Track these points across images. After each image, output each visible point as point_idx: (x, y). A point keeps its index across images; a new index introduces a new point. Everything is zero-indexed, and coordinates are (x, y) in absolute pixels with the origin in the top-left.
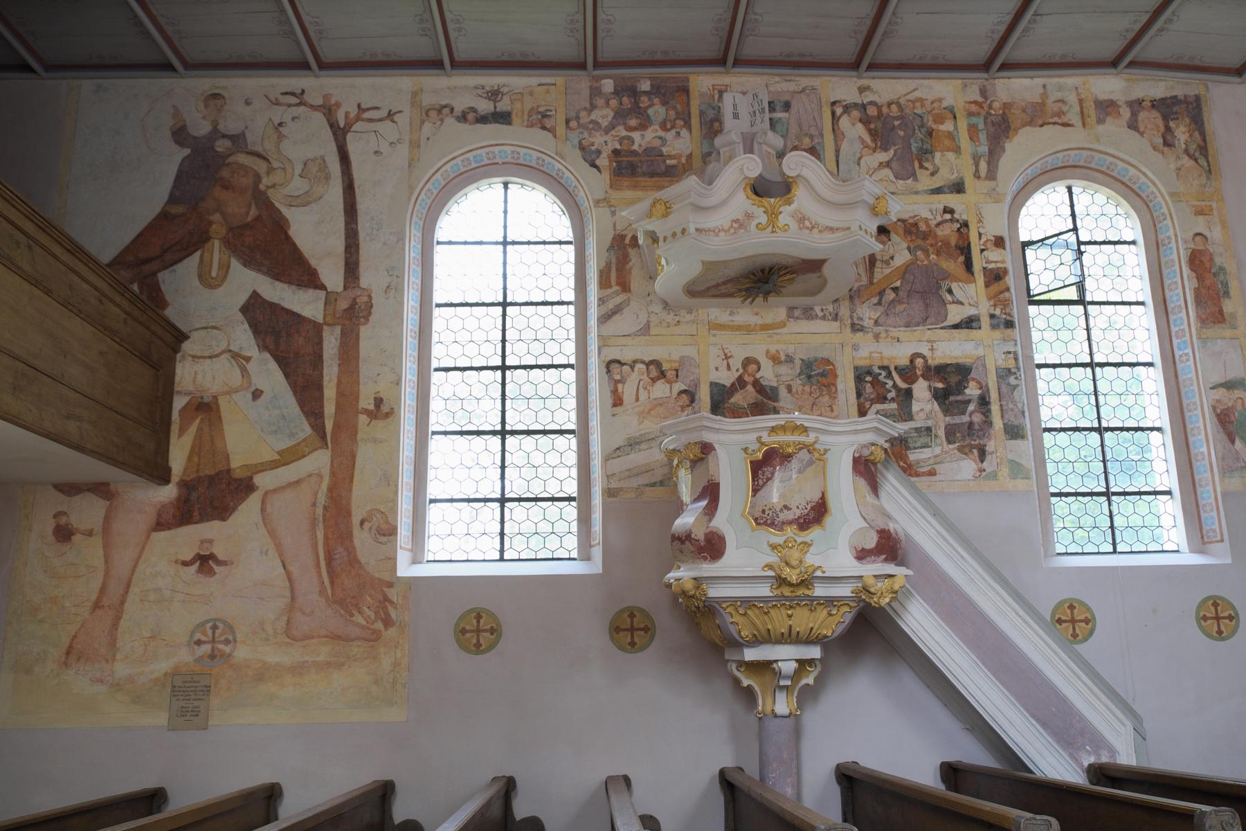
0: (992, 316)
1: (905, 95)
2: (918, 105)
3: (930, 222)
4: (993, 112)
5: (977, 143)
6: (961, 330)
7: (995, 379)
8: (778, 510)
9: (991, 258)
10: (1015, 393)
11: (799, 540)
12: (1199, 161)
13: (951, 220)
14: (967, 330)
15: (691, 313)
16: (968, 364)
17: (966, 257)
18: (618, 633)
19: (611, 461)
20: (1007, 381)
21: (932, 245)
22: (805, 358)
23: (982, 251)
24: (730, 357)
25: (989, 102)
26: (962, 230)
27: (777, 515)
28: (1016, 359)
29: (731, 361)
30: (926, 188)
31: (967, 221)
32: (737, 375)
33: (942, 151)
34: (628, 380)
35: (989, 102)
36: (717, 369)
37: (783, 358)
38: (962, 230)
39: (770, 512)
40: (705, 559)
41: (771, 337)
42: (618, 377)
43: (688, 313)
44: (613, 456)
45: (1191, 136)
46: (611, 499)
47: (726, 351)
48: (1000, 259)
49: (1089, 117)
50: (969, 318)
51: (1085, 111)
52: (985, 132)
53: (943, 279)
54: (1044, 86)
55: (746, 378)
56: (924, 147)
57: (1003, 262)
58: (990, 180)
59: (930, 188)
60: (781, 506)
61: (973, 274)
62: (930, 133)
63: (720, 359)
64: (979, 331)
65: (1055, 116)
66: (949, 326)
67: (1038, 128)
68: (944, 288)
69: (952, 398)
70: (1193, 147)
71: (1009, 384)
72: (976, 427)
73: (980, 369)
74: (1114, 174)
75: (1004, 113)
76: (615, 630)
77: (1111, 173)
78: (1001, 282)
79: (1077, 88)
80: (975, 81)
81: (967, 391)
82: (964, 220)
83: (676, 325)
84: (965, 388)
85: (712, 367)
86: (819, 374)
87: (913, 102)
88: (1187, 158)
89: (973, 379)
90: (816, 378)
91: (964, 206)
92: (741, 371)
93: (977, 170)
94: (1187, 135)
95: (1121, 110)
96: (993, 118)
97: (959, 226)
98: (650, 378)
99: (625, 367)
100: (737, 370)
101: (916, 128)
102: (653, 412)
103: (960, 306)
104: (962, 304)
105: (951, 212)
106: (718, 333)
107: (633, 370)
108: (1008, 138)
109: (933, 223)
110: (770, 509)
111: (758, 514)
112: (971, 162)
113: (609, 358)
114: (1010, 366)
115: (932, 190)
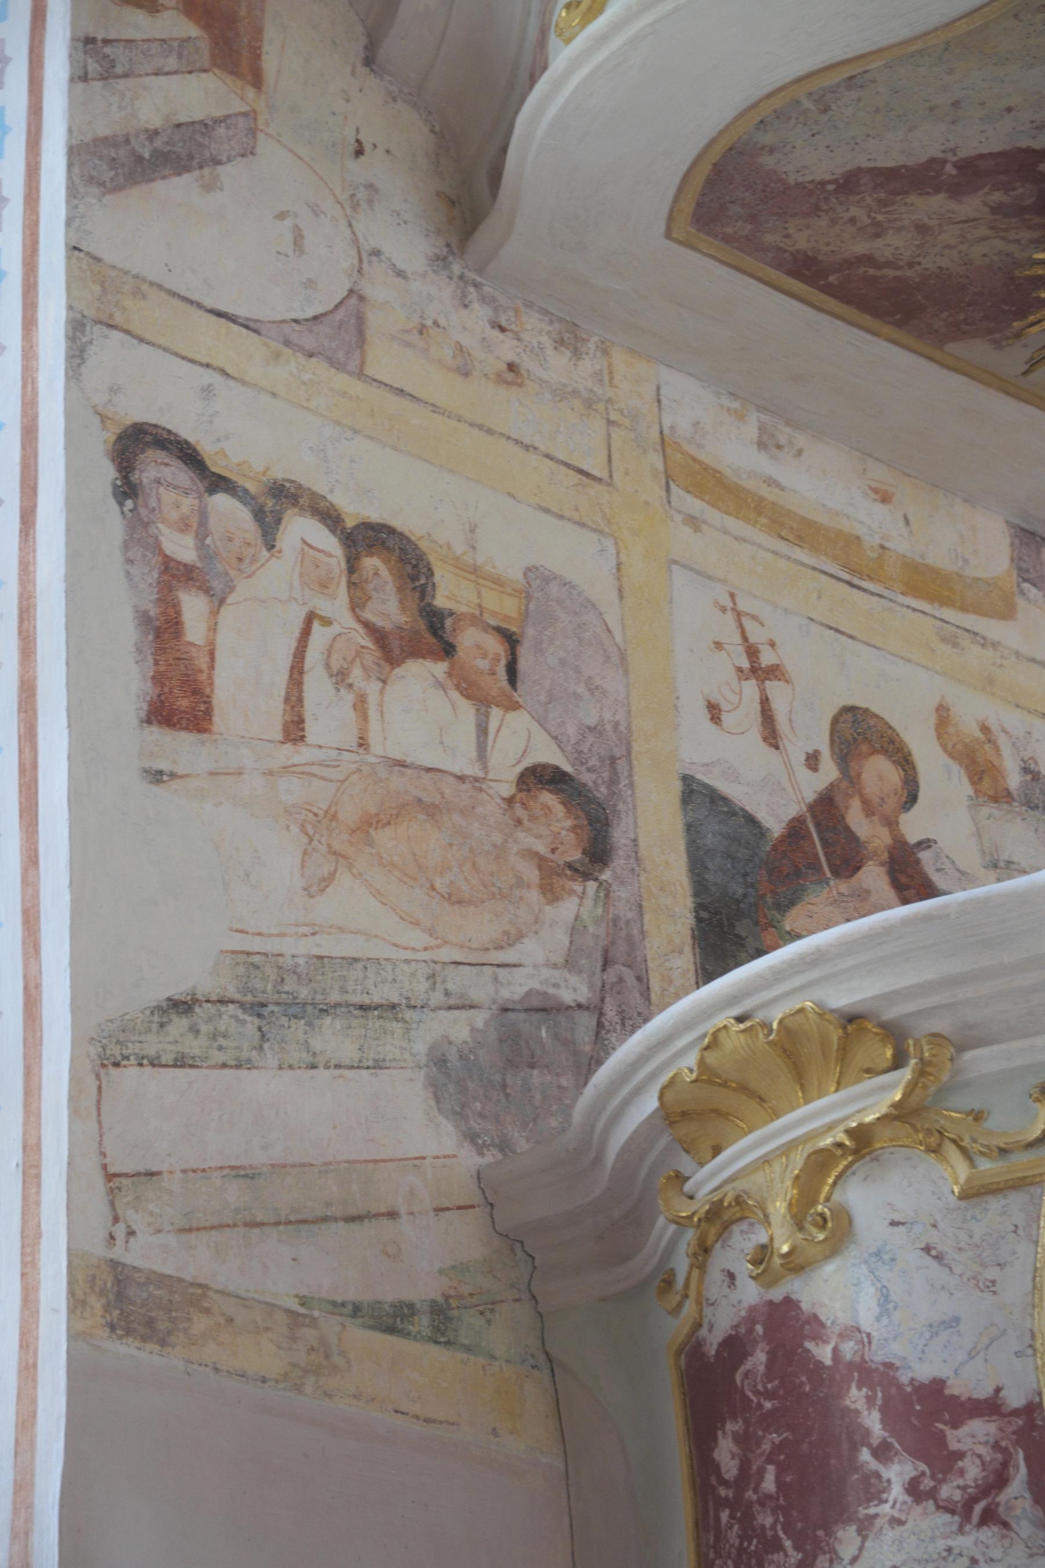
15: (577, 354)
19: (130, 1076)
29: (774, 688)
36: (714, 713)
37: (1014, 780)
41: (951, 641)
43: (560, 342)
44: (152, 1045)
46: (127, 1349)
47: (756, 635)
83: (500, 379)
92: (829, 772)
98: (367, 625)
99: (221, 501)
100: (812, 761)
102: (384, 837)
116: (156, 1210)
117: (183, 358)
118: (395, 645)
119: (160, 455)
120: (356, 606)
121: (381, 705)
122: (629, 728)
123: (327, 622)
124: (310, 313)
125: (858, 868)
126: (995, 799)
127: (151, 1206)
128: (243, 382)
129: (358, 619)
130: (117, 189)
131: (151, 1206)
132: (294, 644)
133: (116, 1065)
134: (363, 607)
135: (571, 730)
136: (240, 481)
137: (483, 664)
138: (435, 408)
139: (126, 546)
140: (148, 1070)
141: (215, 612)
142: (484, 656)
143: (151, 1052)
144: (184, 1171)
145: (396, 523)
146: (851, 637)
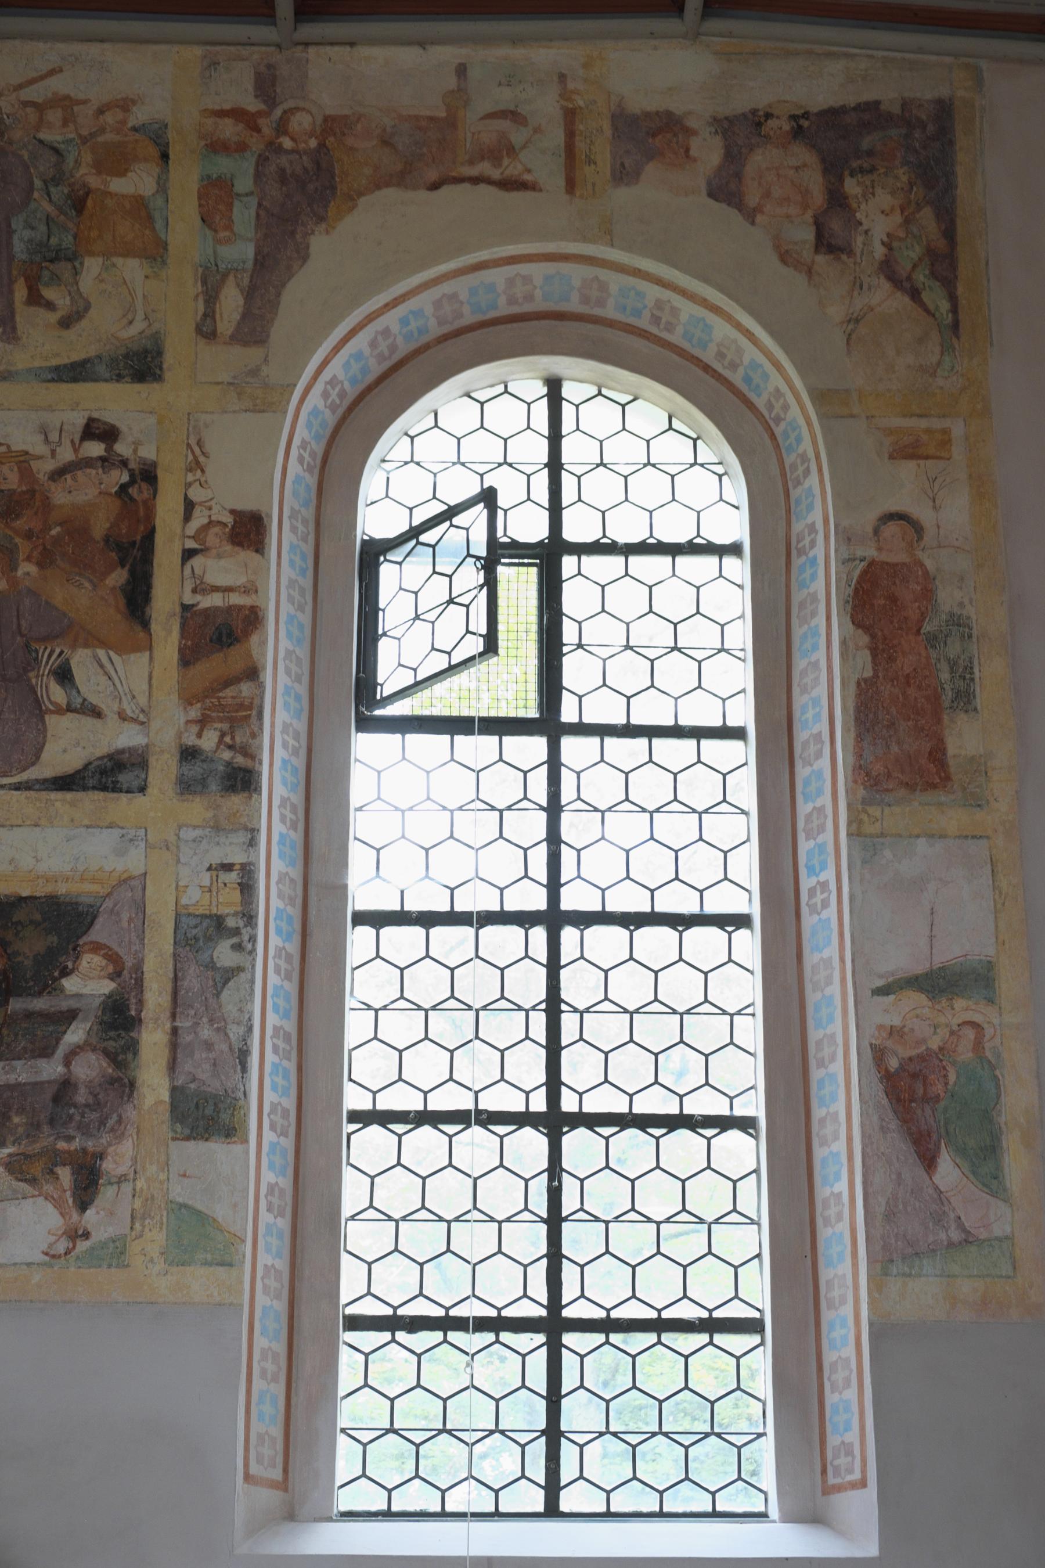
0: (189, 754)
1: (20, 87)
2: (54, 116)
3: (35, 465)
4: (287, 143)
5: (223, 234)
6: (80, 795)
7: (169, 949)
9: (211, 579)
10: (225, 994)
12: (925, 296)
13: (103, 459)
14: (100, 795)
16: (83, 899)
17: (132, 573)
20: (205, 957)
21: (29, 535)
23: (188, 554)
25: (278, 112)
26: (133, 491)
28: (247, 888)
30: (37, 364)
31: (154, 465)
33: (107, 254)
35: (278, 112)
38: (133, 491)
45: (907, 221)
48: (241, 580)
49: (590, 161)
50: (110, 757)
51: (580, 145)
52: (254, 201)
53: (45, 639)
54: (461, 70)
56: (54, 241)
57: (250, 589)
58: (245, 344)
59: (54, 362)
61: (145, 624)
62: (79, 201)
64: (139, 799)
65: (483, 158)
66: (45, 781)
67: (423, 195)
68: (48, 661)
69: (16, 1004)
70: (910, 254)
71: (211, 966)
72: (82, 1097)
73: (125, 916)
74: (675, 338)
75: (322, 145)
77: (665, 335)
78: (235, 651)
79: (562, 78)
80: (245, 51)
81: (70, 984)
82: (143, 462)
84: (65, 973)
87: (40, 108)
88: (886, 285)
89: (97, 948)
91: (152, 420)
93: (209, 314)
94: (898, 218)
95: (695, 144)
96: (284, 161)
97: (125, 478)
101: (38, 183)
103: (89, 722)
104: (96, 713)
105: (109, 434)
108: (321, 219)
109: (43, 468)
112: (193, 287)
114: (223, 910)
115: (57, 369)
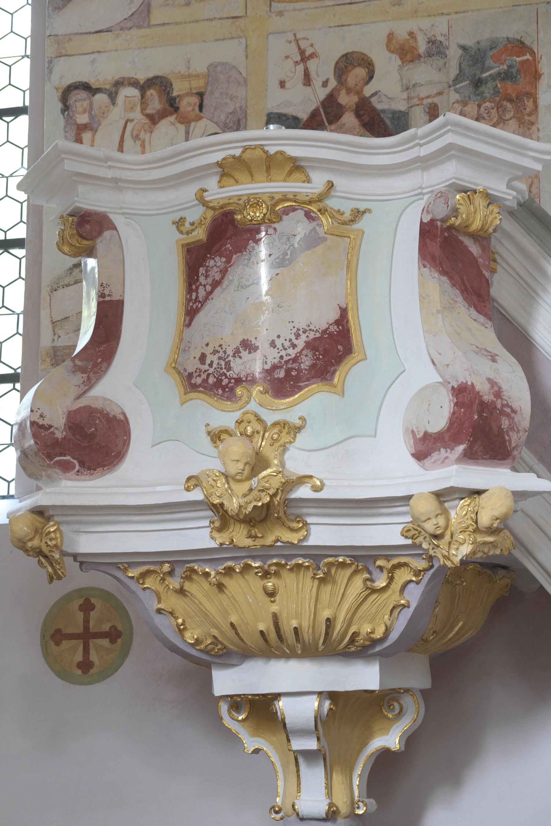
8: (230, 352)
11: (270, 418)
18: (57, 644)
19: (60, 292)
22: (469, 42)
24: (313, 55)
27: (228, 364)
32: (323, 94)
34: (104, 123)
36: (282, 84)
39: (215, 358)
40: (66, 467)
42: (82, 119)
55: (344, 99)
60: (237, 343)
63: (290, 62)
76: (53, 637)
85: (273, 83)
86: (499, 74)
90: (490, 85)
92: (333, 83)
99: (98, 96)
100: (325, 84)
106: (289, 6)
107: (114, 103)
110: (215, 352)
111: (192, 365)
113: (68, 81)
116: (67, 328)
117: (85, 54)
118: (156, 118)
119: (77, 91)
120: (142, 110)
121: (150, 141)
122: (246, 106)
123: (132, 121)
124: (130, 13)
125: (340, 117)
126: (412, 61)
127: (65, 327)
128: (105, 52)
129: (144, 114)
130: (64, 6)
131: (65, 327)
132: (121, 133)
133: (56, 290)
134: (145, 109)
135: (223, 117)
136: (103, 86)
137: (189, 109)
138: (176, 23)
139: (65, 127)
140: (66, 288)
141: (93, 136)
142: (190, 106)
143: (67, 282)
144: (77, 314)
145: (160, 74)
146: (349, 25)
